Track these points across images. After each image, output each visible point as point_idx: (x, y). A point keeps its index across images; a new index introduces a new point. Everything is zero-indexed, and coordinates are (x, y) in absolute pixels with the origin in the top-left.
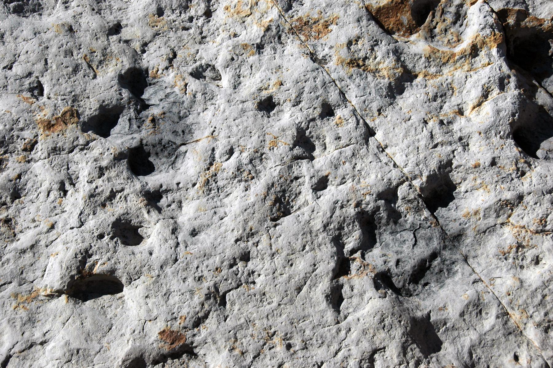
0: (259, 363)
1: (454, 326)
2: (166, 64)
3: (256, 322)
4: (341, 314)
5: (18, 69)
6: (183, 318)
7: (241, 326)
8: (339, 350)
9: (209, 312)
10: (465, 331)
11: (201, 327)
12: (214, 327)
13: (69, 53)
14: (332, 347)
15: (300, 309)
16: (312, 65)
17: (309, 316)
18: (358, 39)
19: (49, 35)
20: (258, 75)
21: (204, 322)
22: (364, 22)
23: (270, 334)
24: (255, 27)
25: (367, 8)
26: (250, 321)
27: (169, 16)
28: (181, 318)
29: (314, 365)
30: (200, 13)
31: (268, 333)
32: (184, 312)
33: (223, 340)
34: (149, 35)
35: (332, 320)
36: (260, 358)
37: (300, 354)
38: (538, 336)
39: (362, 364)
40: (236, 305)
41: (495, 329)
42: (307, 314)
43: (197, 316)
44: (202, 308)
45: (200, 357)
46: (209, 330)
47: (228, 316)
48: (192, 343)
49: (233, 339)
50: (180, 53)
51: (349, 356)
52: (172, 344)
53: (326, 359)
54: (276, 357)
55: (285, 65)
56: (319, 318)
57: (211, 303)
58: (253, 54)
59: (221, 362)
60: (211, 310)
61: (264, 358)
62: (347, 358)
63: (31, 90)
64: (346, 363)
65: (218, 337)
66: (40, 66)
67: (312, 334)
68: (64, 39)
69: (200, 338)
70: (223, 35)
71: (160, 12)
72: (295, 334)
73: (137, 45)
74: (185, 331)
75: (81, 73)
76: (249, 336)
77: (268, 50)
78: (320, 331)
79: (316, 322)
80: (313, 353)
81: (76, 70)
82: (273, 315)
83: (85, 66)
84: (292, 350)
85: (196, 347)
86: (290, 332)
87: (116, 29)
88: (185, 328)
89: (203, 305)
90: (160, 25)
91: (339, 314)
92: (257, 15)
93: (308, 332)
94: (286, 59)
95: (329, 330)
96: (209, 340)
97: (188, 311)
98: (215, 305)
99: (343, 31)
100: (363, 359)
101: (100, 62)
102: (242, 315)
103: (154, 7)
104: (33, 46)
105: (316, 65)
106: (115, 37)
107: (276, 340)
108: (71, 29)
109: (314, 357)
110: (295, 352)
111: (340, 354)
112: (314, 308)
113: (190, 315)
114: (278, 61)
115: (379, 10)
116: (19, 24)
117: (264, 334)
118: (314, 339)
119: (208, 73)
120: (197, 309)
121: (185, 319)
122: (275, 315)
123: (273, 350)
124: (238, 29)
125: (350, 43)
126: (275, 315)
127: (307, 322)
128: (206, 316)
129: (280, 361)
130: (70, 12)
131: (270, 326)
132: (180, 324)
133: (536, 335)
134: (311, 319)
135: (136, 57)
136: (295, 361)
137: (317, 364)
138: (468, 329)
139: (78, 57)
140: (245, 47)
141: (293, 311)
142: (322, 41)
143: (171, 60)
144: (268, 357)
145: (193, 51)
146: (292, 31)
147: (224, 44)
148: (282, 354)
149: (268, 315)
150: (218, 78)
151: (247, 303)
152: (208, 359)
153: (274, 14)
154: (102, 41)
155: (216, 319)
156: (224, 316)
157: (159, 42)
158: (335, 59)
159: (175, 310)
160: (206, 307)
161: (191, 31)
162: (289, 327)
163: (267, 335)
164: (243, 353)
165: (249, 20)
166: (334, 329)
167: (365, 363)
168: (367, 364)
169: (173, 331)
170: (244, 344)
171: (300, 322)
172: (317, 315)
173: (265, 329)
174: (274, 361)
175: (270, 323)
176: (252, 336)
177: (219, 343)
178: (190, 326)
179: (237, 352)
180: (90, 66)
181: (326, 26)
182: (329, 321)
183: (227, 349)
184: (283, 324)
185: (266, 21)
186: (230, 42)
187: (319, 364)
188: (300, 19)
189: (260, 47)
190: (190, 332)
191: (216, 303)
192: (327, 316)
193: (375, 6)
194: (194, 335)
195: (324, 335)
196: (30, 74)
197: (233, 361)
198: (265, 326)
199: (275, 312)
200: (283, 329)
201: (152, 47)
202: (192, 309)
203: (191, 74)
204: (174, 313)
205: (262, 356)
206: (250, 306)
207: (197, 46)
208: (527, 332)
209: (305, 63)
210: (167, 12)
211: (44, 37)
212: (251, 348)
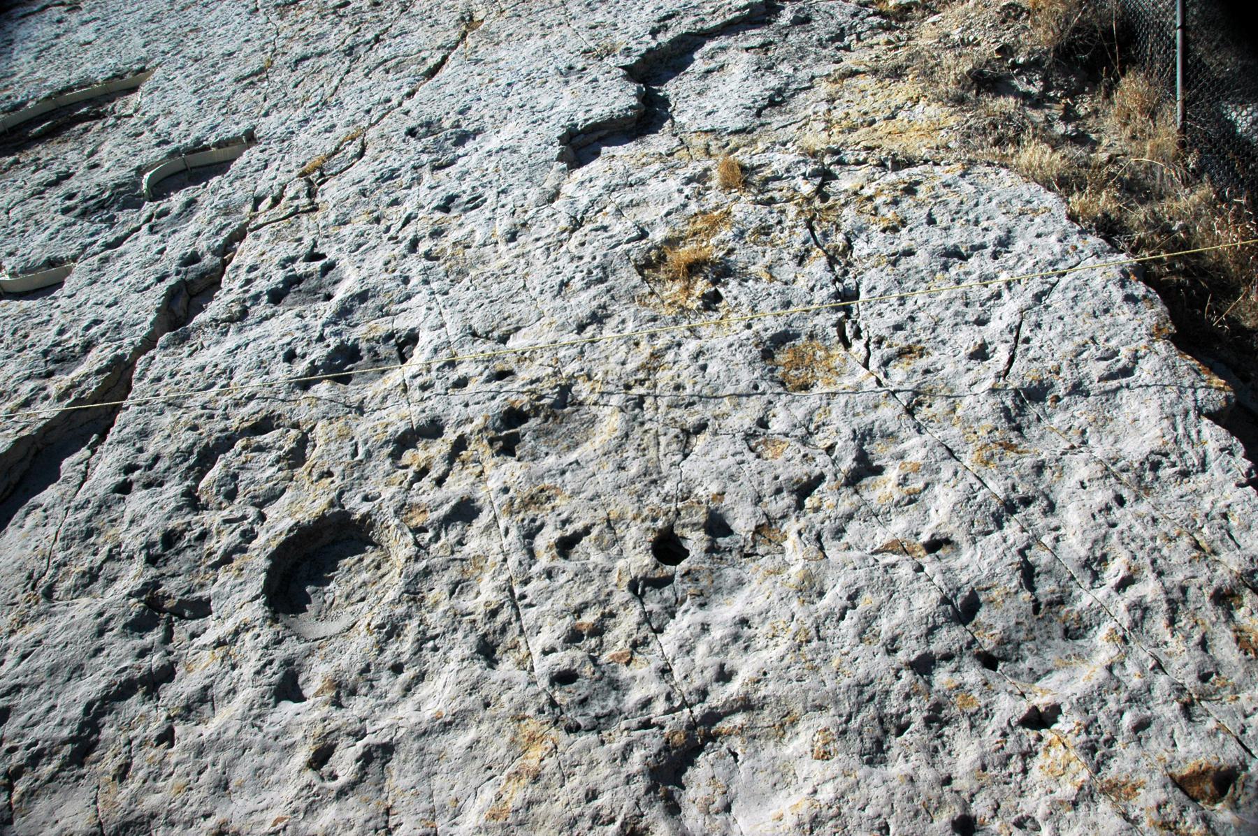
2: (992, 813)
5: (870, 811)
13: (911, 799)
16: (1126, 824)
18: (1166, 803)
19: (895, 783)
20: (1075, 830)
22: (1170, 788)
24: (1069, 786)
25: (1171, 776)
27: (992, 772)
30: (1018, 770)
34: (976, 787)
50: (1002, 804)
55: (1100, 822)
58: (1069, 810)
63: (880, 829)
66: (887, 809)
68: (906, 787)
70: (1039, 791)
71: (984, 768)
73: (965, 795)
75: (921, 817)
77: (1082, 807)
81: (917, 814)
83: (923, 811)
87: (948, 781)
90: (984, 779)
92: (1070, 775)
94: (1100, 817)
99: (1151, 795)
101: (936, 809)
103: (979, 763)
104: (882, 791)
105: (1129, 824)
106: (947, 788)
108: (912, 780)
114: (1092, 818)
115: (1182, 778)
116: (871, 774)
119: (1028, 824)
124: (1053, 787)
125: (1159, 807)
130: (910, 764)
135: (966, 806)
139: (918, 803)
140: (1062, 802)
142: (1132, 802)
143: (995, 810)
145: (1014, 803)
146: (1102, 791)
147: (1043, 799)
150: (1038, 828)
153: (1085, 775)
154: (937, 791)
157: (984, 794)
158: (1146, 820)
161: (1012, 785)
165: (1062, 779)
180: (928, 812)
181: (1134, 789)
185: (1079, 780)
186: (1048, 798)
188: (1109, 781)
189: (1075, 804)
193: (1178, 775)
196: (879, 816)
201: (979, 798)
203: (1014, 824)
207: (1018, 800)
209: (1118, 822)
210: (990, 768)
211: (891, 785)
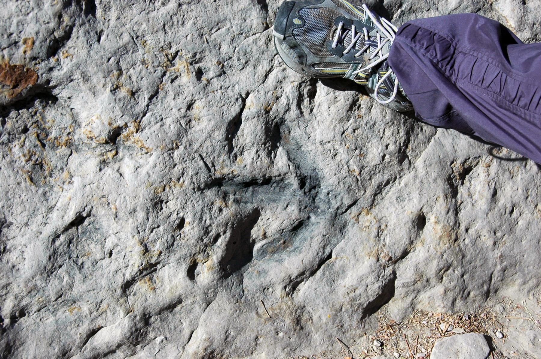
0: (159, 106)
1: (411, 8)
3: (148, 37)
4: (270, 11)
6: (30, 42)
7: (125, 47)
8: (270, 71)
9: (71, 29)
10: (425, 12)
11: (61, 54)
12: (83, 53)
14: (260, 68)
15: (210, 9)
17: (225, 20)
21: (63, 45)
23: (170, 57)
26: (137, 37)
28: (25, 42)
29: (237, 99)
31: (167, 55)
32: (30, 30)
33: (101, 75)
35: (258, 24)
36: (159, 98)
37: (216, 84)
38: (516, 11)
39: (302, 88)
40: (113, 10)
41: (462, 6)
42: (222, 17)
43: (52, 36)
44: (60, 23)
45: (61, 101)
46: (75, 61)
47: (102, 31)
48: (48, 81)
49: (115, 73)
51: (284, 78)
52: (15, 87)
53: (253, 88)
54: (182, 93)
56: (240, 22)
57: (74, 13)
59: (100, 110)
60: (74, 25)
61: (165, 97)
62: (281, 82)
64: (280, 90)
65: (91, 70)
67: (232, 51)
69: (62, 72)
72: (207, 52)
74: (36, 64)
76: (139, 63)
78: (243, 43)
79: (236, 30)
80: (234, 79)
82: (173, 24)
84: (204, 79)
85: (55, 87)
86: (199, 51)
88: (34, 58)
89: (60, 16)
91: (267, 11)
93: (225, 48)
95: (255, 41)
96: (77, 76)
97: (36, 29)
98: (79, 16)
100: (303, 82)
102: (124, 28)
107: (180, 65)
109: (236, 87)
110: (209, 81)
111: (271, 76)
112: (232, 5)
113: (41, 36)
117: (162, 58)
118: (235, 58)
120: (52, 25)
121: (33, 43)
122: (175, 23)
123: (176, 83)
126: (175, 23)
127: (223, 30)
128: (67, 36)
129: (189, 98)
131: (170, 43)
132: (25, 52)
133: (513, 10)
134: (228, 25)
136: (210, 97)
137: (241, 96)
138: (428, 10)
141: (202, 14)
144: (171, 94)
148: (191, 88)
149: (164, 25)
151: (129, 7)
152: (76, 104)
155: (84, 40)
156: (96, 32)
159: (13, 28)
160: (66, 19)
162: (198, 42)
163: (166, 59)
164: (133, 94)
166: (262, 38)
167: (306, 86)
168: (308, 88)
169: (15, 66)
170: (134, 79)
171: (213, 31)
172: (237, 18)
173: (162, 49)
174: (180, 100)
175: (169, 38)
176: (143, 62)
177: (94, 80)
178: (43, 54)
179: (123, 93)
182: (254, 26)
183: (108, 90)
184: (189, 37)
187: (244, 96)
190: (43, 64)
191: (81, 10)
192: (252, 18)
194: (51, 69)
195: (249, 49)
197: (121, 108)
198: (162, 44)
199: (175, 19)
200: (190, 47)
202: (44, 26)
204: (11, 34)
205: (161, 95)
206: (135, 11)
208: (500, 5)
212: (144, 83)
